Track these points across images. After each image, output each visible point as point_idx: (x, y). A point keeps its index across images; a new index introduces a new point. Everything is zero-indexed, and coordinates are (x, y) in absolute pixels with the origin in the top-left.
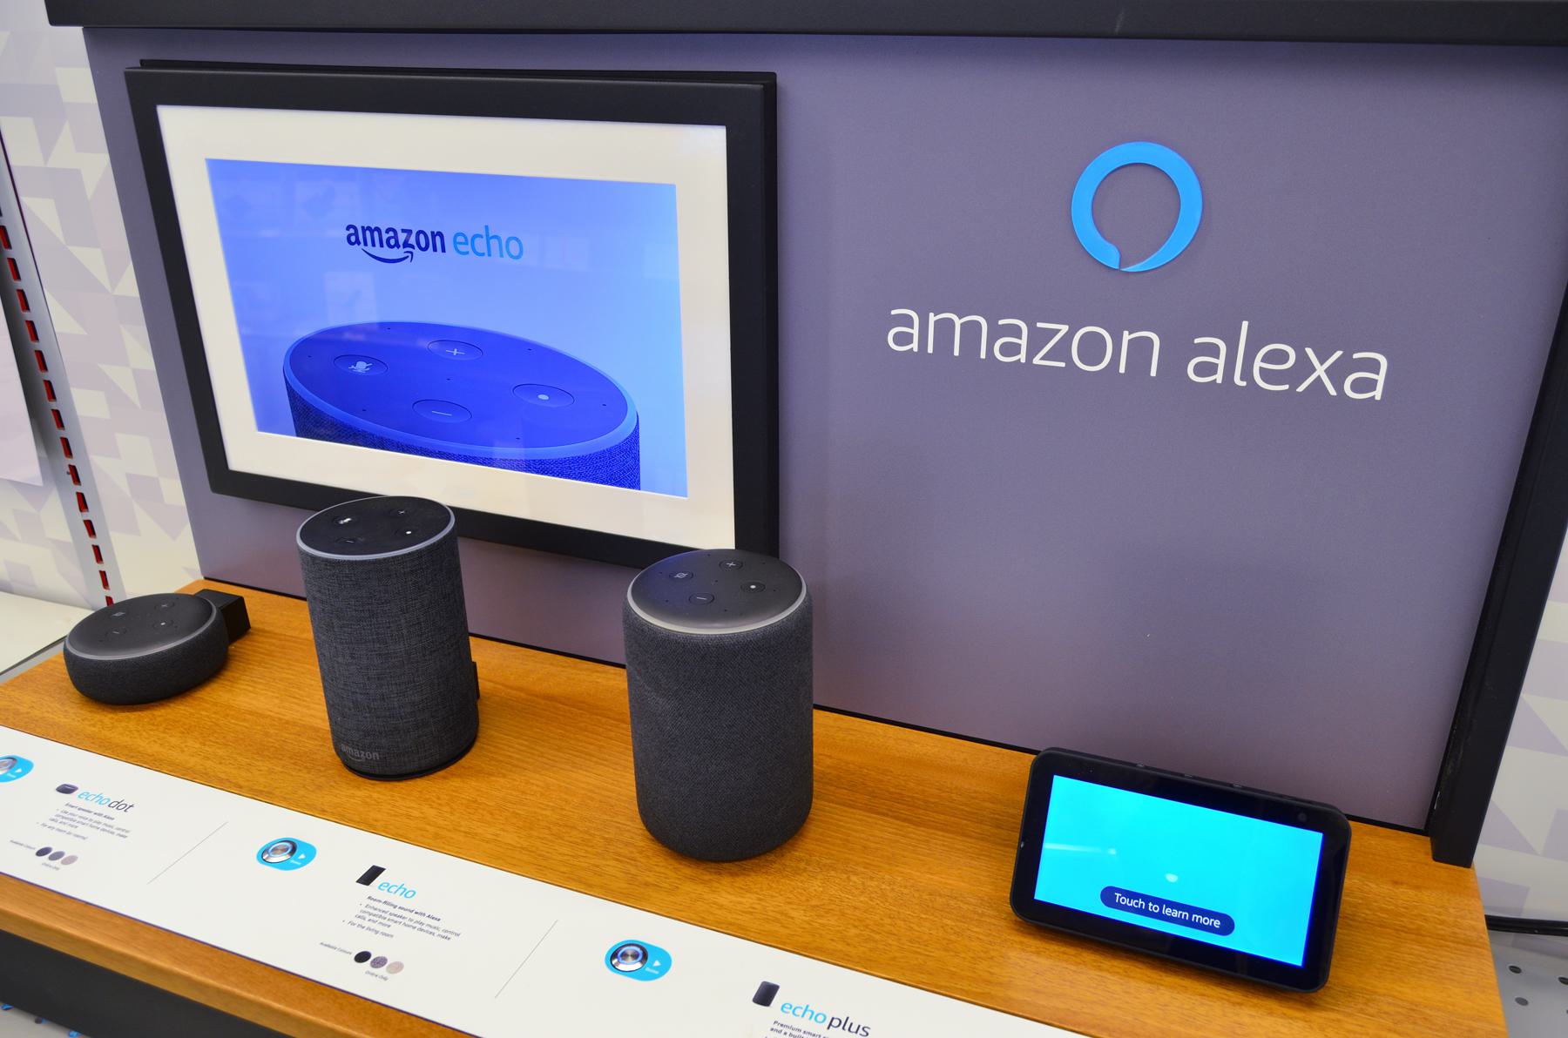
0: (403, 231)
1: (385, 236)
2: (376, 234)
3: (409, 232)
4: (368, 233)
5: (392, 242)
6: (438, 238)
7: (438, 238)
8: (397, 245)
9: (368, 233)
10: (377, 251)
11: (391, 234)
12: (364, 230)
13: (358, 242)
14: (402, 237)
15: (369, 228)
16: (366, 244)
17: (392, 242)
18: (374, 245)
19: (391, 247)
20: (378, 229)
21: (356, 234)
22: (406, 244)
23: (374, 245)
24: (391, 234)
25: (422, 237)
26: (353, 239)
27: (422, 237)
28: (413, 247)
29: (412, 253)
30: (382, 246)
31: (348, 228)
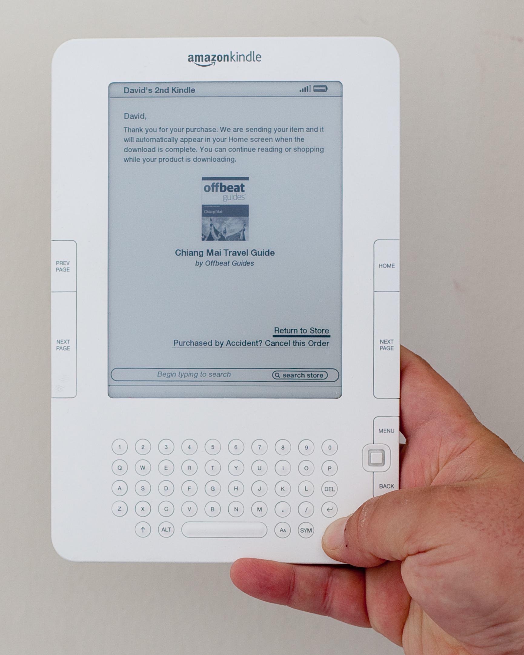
0: (212, 55)
1: (204, 58)
2: (201, 57)
3: (215, 56)
4: (197, 57)
5: (207, 59)
6: (226, 57)
7: (226, 57)
8: (209, 60)
9: (197, 57)
10: (201, 63)
11: (207, 57)
12: (196, 56)
13: (193, 60)
14: (211, 58)
15: (198, 56)
16: (196, 61)
17: (207, 59)
18: (199, 61)
19: (206, 61)
20: (202, 56)
21: (192, 58)
22: (213, 60)
23: (199, 61)
24: (207, 57)
25: (220, 57)
26: (191, 60)
27: (220, 57)
28: (215, 60)
29: (215, 63)
30: (202, 61)
31: (189, 56)
